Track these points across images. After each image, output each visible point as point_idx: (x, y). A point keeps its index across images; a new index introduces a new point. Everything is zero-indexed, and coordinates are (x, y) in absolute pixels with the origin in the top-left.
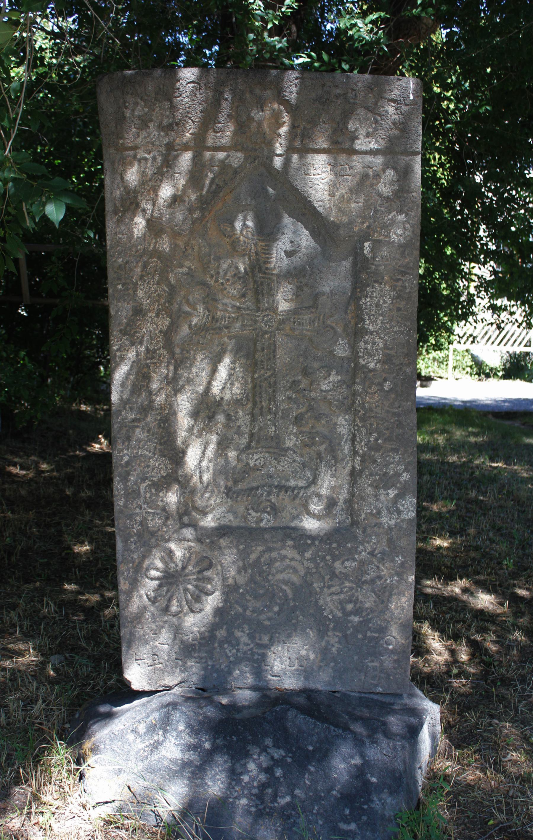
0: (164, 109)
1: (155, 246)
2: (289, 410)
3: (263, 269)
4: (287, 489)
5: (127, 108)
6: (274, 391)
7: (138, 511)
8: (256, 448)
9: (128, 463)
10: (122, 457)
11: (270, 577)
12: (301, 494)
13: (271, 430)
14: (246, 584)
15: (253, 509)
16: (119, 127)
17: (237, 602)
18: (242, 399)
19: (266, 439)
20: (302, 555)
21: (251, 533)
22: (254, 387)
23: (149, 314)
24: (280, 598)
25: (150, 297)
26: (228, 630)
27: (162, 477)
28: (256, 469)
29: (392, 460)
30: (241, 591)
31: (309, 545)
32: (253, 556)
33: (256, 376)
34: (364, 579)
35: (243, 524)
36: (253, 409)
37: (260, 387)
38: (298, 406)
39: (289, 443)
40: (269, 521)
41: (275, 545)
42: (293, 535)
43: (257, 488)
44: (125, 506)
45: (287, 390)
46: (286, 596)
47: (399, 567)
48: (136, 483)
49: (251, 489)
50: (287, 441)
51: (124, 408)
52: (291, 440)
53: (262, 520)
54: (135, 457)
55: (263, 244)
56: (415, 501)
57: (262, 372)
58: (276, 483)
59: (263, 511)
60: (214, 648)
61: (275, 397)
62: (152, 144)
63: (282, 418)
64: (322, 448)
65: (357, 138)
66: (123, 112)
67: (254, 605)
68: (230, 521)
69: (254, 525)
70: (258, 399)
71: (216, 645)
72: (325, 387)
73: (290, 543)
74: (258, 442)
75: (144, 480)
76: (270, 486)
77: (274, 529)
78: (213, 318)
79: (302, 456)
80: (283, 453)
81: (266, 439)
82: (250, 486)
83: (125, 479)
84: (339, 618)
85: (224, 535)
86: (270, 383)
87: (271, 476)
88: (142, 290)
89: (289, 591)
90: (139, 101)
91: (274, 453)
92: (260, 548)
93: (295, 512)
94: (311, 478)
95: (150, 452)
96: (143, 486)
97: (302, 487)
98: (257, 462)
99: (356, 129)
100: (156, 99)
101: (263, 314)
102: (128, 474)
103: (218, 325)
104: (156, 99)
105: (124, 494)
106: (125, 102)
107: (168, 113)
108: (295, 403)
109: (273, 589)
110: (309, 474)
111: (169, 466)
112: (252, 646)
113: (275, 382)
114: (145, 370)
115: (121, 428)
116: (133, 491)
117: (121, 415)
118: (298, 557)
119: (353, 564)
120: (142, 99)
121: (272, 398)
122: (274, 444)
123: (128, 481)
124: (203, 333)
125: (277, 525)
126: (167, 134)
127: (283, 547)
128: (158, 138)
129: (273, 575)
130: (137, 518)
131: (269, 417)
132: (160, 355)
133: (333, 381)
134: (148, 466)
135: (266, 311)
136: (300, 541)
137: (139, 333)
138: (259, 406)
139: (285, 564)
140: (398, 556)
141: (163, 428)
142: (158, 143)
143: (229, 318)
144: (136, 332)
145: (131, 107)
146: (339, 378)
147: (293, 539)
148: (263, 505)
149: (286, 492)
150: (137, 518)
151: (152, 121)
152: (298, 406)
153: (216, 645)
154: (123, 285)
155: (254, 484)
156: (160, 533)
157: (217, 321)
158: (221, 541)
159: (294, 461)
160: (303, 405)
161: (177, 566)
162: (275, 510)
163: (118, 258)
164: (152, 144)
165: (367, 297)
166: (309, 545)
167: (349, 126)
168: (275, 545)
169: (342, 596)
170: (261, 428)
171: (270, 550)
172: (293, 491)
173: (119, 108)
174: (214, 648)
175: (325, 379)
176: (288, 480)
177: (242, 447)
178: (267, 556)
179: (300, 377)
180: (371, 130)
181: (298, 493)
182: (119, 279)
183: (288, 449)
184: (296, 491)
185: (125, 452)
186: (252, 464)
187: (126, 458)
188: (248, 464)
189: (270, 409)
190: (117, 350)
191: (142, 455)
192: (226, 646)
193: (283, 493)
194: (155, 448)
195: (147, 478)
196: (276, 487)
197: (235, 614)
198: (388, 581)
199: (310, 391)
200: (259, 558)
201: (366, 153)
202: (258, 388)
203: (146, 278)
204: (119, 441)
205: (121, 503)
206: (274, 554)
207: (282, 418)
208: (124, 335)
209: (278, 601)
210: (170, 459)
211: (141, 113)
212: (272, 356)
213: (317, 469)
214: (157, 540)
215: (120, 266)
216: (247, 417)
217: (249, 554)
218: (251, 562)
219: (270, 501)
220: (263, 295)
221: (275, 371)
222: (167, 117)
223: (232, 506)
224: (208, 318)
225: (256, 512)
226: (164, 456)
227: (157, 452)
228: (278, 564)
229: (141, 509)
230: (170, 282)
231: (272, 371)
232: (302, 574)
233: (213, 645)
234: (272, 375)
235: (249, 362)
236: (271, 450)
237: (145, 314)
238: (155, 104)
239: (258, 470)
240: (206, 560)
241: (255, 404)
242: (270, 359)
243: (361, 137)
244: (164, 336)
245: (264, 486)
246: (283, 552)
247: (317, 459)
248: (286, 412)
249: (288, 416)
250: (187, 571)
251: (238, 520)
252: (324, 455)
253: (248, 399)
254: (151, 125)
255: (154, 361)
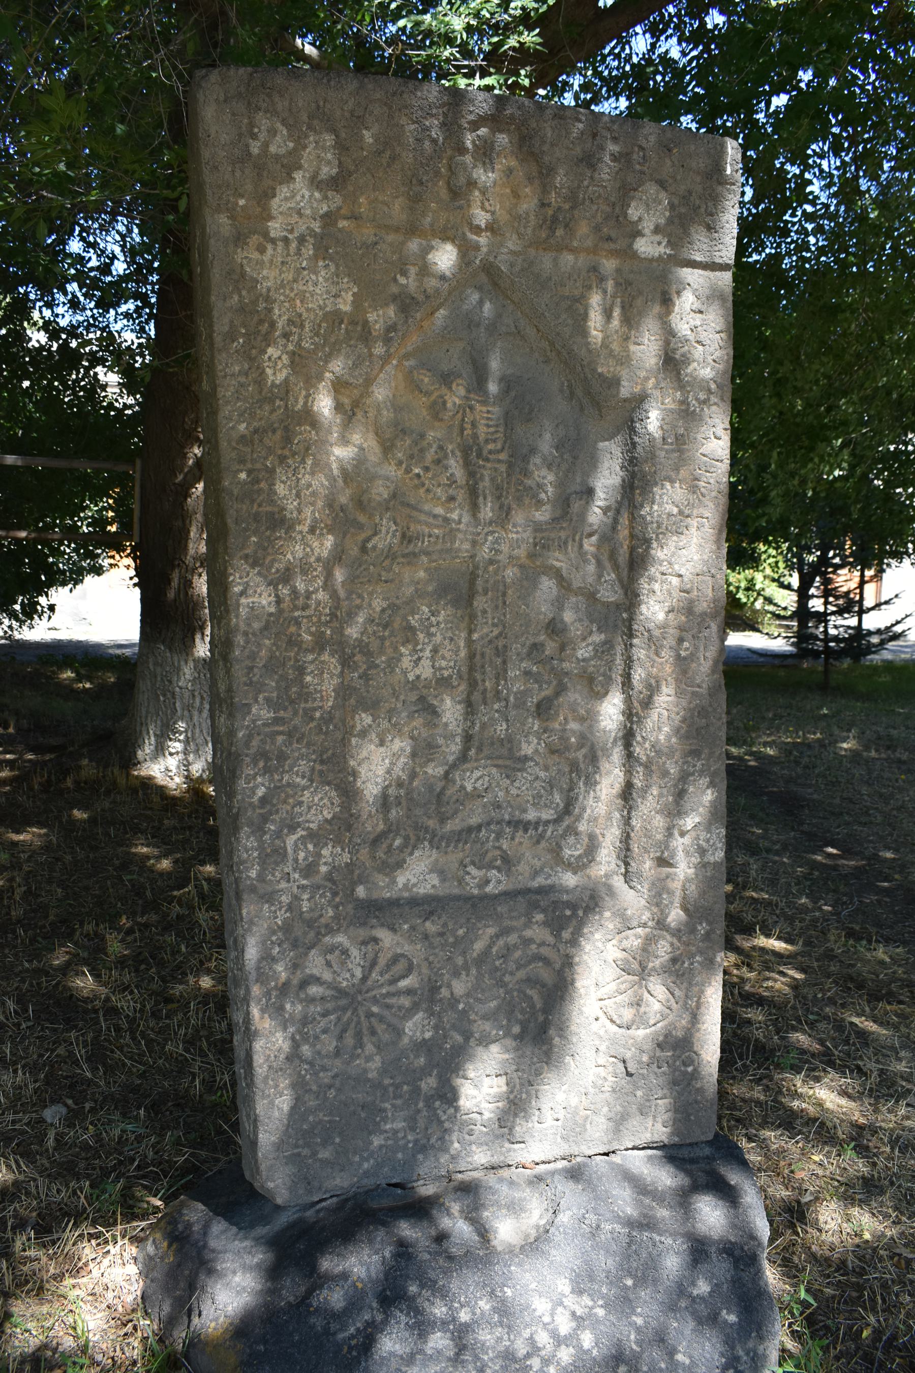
0: (324, 148)
1: (306, 403)
2: (525, 693)
3: (485, 452)
4: (526, 826)
5: (254, 136)
6: (504, 662)
7: (283, 885)
8: (476, 760)
9: (264, 800)
10: (253, 791)
11: (507, 978)
12: (549, 833)
13: (501, 728)
14: (468, 995)
15: (473, 863)
16: (238, 174)
17: (454, 1027)
18: (450, 677)
19: (493, 744)
20: (558, 936)
21: (474, 906)
22: (471, 656)
23: (298, 528)
24: (523, 1011)
25: (298, 495)
26: (440, 1077)
27: (326, 820)
28: (477, 795)
29: (691, 769)
30: (461, 1006)
31: (569, 918)
32: (479, 946)
33: (475, 636)
34: (651, 965)
35: (456, 891)
36: (470, 694)
37: (483, 655)
38: (541, 686)
39: (527, 749)
40: (499, 882)
41: (515, 923)
42: (542, 903)
43: (479, 827)
44: (261, 878)
45: (522, 660)
46: (533, 1006)
47: (702, 941)
48: (278, 835)
49: (470, 830)
50: (524, 746)
51: (256, 701)
52: (529, 743)
53: (488, 882)
54: (276, 787)
55: (484, 409)
56: (723, 831)
57: (485, 631)
58: (507, 817)
59: (490, 866)
60: (419, 1111)
61: (506, 671)
62: (299, 213)
63: (516, 707)
64: (580, 755)
65: (639, 234)
66: (247, 146)
67: (482, 1028)
68: (433, 886)
69: (476, 892)
70: (478, 676)
71: (421, 1105)
72: (581, 653)
73: (539, 917)
74: (480, 750)
75: (292, 828)
76: (498, 823)
77: (508, 895)
78: (404, 536)
79: (546, 768)
80: (518, 766)
81: (493, 744)
82: (465, 824)
83: (259, 830)
84: (615, 1034)
85: (432, 913)
86: (497, 648)
87: (498, 806)
88: (282, 482)
89: (536, 998)
90: (279, 126)
91: (506, 767)
92: (491, 931)
93: (537, 863)
94: (562, 805)
95: (303, 777)
96: (291, 840)
97: (547, 822)
98: (478, 785)
99: (640, 219)
100: (310, 127)
101: (486, 530)
102: (265, 819)
103: (411, 547)
104: (310, 127)
105: (259, 857)
106: (251, 125)
107: (329, 156)
108: (536, 681)
109: (513, 997)
110: (557, 798)
111: (337, 801)
112: (478, 1099)
113: (505, 647)
114: (293, 629)
115: (250, 737)
116: (275, 851)
117: (249, 713)
118: (550, 939)
119: (636, 943)
120: (284, 122)
121: (502, 674)
122: (504, 751)
123: (265, 833)
124: (387, 563)
125: (511, 887)
126: (326, 197)
127: (528, 924)
128: (310, 202)
129: (512, 974)
130: (284, 898)
131: (496, 707)
132: (318, 603)
133: (593, 643)
134: (300, 803)
135: (490, 523)
136: (554, 912)
137: (280, 561)
138: (481, 688)
139: (530, 953)
140: (701, 923)
141: (326, 733)
142: (308, 212)
143: (430, 536)
144: (274, 561)
145: (262, 136)
146: (603, 636)
147: (544, 911)
148: (490, 855)
149: (526, 830)
150: (284, 898)
151: (300, 167)
152: (541, 686)
153: (421, 1105)
154: (249, 472)
155: (474, 821)
156: (323, 920)
157: (410, 541)
158: (428, 924)
159: (537, 778)
160: (549, 683)
161: (353, 976)
162: (508, 863)
163: (239, 422)
164: (299, 213)
165: (653, 503)
166: (569, 918)
167: (630, 211)
168: (515, 923)
169: (620, 998)
170: (484, 726)
171: (505, 932)
172: (536, 829)
173: (240, 135)
174: (419, 1111)
175: (584, 639)
176: (525, 811)
177: (451, 758)
178: (501, 942)
179: (542, 638)
180: (662, 221)
181: (545, 831)
182: (242, 461)
183: (526, 758)
184: (541, 829)
185: (259, 780)
186: (469, 788)
187: (261, 791)
188: (463, 788)
189: (498, 692)
190: (243, 593)
191: (288, 784)
192: (437, 1103)
193: (520, 833)
194: (313, 769)
195: (299, 825)
196: (509, 823)
197: (452, 1047)
198: (686, 965)
199: (562, 660)
200: (490, 947)
201: (652, 260)
202: (478, 657)
203: (290, 461)
204: (248, 759)
205: (253, 874)
206: (513, 939)
207: (516, 707)
208: (253, 566)
209: (520, 1016)
210: (338, 788)
211: (282, 151)
212: (500, 603)
213: (571, 789)
214: (318, 933)
215: (243, 437)
216: (459, 707)
217: (472, 943)
218: (475, 955)
219: (500, 848)
220: (485, 498)
221: (504, 626)
222: (329, 163)
223: (437, 860)
224: (394, 536)
225: (479, 868)
226: (329, 784)
227: (316, 776)
228: (518, 954)
229: (288, 881)
230: (331, 470)
231: (500, 628)
232: (557, 966)
233: (416, 1105)
234: (500, 634)
235: (459, 613)
236: (500, 762)
237: (290, 528)
238: (307, 137)
239: (479, 796)
240: (403, 960)
241: (473, 685)
242: (497, 607)
243: (647, 231)
244: (324, 567)
245: (488, 824)
246: (528, 933)
247: (571, 772)
248: (521, 697)
249: (525, 703)
250: (369, 983)
251: (447, 884)
252: (582, 766)
253: (461, 677)
254: (298, 175)
255: (307, 613)
